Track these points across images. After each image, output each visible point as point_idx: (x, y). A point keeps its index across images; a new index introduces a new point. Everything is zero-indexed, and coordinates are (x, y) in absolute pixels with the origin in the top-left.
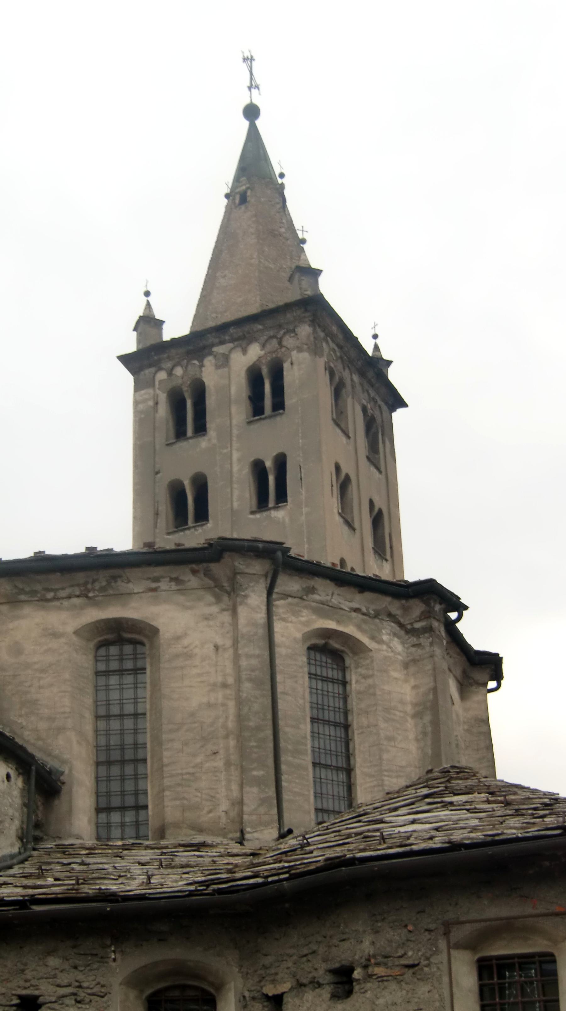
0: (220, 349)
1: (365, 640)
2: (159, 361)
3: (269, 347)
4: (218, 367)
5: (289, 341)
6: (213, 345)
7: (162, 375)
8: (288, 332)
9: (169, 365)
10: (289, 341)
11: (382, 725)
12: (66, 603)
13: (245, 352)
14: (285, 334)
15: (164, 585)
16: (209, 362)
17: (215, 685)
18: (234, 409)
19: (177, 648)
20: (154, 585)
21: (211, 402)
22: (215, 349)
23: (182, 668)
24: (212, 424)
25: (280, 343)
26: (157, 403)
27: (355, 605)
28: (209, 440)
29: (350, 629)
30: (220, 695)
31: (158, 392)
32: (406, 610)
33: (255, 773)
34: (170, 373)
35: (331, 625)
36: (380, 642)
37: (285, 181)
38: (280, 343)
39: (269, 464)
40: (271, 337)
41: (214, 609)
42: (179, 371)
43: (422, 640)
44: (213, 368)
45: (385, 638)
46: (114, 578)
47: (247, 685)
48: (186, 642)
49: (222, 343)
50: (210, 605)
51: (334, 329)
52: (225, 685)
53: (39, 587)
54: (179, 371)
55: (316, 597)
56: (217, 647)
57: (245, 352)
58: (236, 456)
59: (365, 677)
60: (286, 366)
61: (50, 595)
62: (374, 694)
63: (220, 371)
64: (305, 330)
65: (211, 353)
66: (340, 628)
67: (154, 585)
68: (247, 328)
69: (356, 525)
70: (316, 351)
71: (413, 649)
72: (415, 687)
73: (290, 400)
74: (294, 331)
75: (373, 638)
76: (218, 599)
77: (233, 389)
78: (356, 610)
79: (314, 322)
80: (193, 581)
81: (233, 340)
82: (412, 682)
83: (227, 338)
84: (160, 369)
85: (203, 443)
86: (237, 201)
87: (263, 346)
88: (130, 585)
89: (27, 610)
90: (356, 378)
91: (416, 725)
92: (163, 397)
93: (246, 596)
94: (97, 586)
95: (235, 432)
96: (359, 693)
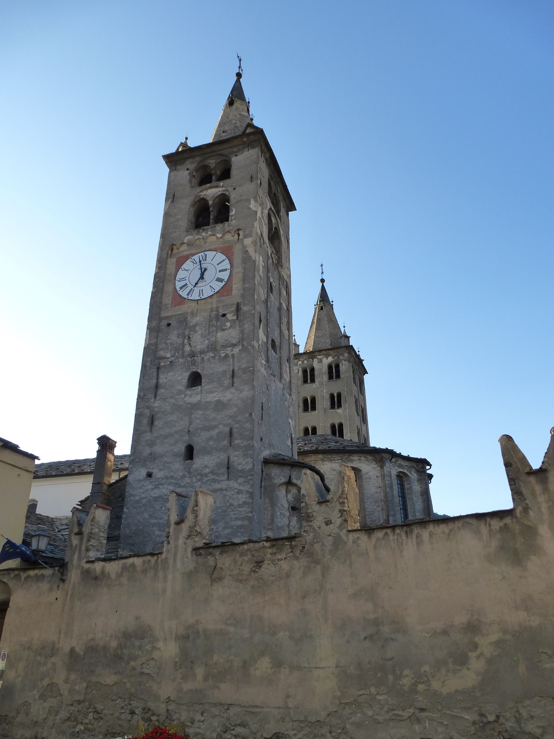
0: (319, 357)
1: (409, 474)
2: (300, 358)
3: (335, 358)
4: (319, 362)
5: (341, 357)
6: (317, 356)
7: (300, 363)
8: (341, 354)
9: (303, 360)
10: (341, 357)
11: (414, 498)
12: (337, 461)
13: (327, 358)
14: (340, 355)
15: (362, 458)
16: (315, 360)
17: (377, 487)
18: (324, 376)
19: (367, 476)
20: (360, 458)
21: (316, 373)
22: (317, 357)
23: (368, 481)
24: (317, 380)
25: (338, 357)
26: (298, 371)
27: (406, 464)
28: (316, 385)
29: (405, 471)
30: (378, 490)
31: (299, 368)
32: (417, 465)
33: (392, 513)
34: (303, 362)
35: (401, 470)
36: (412, 474)
37: (333, 303)
38: (338, 357)
39: (335, 395)
40: (335, 356)
41: (376, 466)
42: (306, 362)
43: (422, 474)
44: (317, 362)
45: (413, 473)
46: (350, 456)
47: (388, 489)
48: (369, 474)
49: (320, 355)
50: (375, 464)
51: (353, 354)
52: (380, 487)
53: (329, 457)
54: (306, 362)
55: (398, 462)
56: (377, 476)
57: (327, 358)
58: (325, 391)
59: (409, 484)
60: (340, 365)
61: (332, 459)
62: (412, 489)
63: (319, 364)
64: (346, 355)
65: (316, 358)
66: (404, 471)
67: (360, 458)
68: (328, 352)
69: (359, 414)
70: (349, 361)
71: (419, 476)
72: (420, 487)
73: (342, 376)
74: (343, 354)
75: (410, 473)
76: (377, 464)
77: (324, 370)
78: (406, 466)
79: (349, 353)
80: (370, 458)
81: (323, 355)
82: (420, 486)
83: (322, 354)
84: (300, 360)
85: (314, 385)
86: (320, 309)
87: (333, 358)
88: (354, 458)
89: (326, 463)
90: (357, 367)
91: (422, 498)
92: (300, 370)
93: (386, 464)
94: (345, 457)
95: (324, 383)
96: (407, 488)
